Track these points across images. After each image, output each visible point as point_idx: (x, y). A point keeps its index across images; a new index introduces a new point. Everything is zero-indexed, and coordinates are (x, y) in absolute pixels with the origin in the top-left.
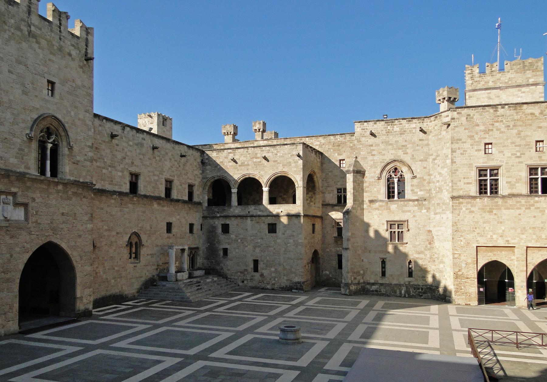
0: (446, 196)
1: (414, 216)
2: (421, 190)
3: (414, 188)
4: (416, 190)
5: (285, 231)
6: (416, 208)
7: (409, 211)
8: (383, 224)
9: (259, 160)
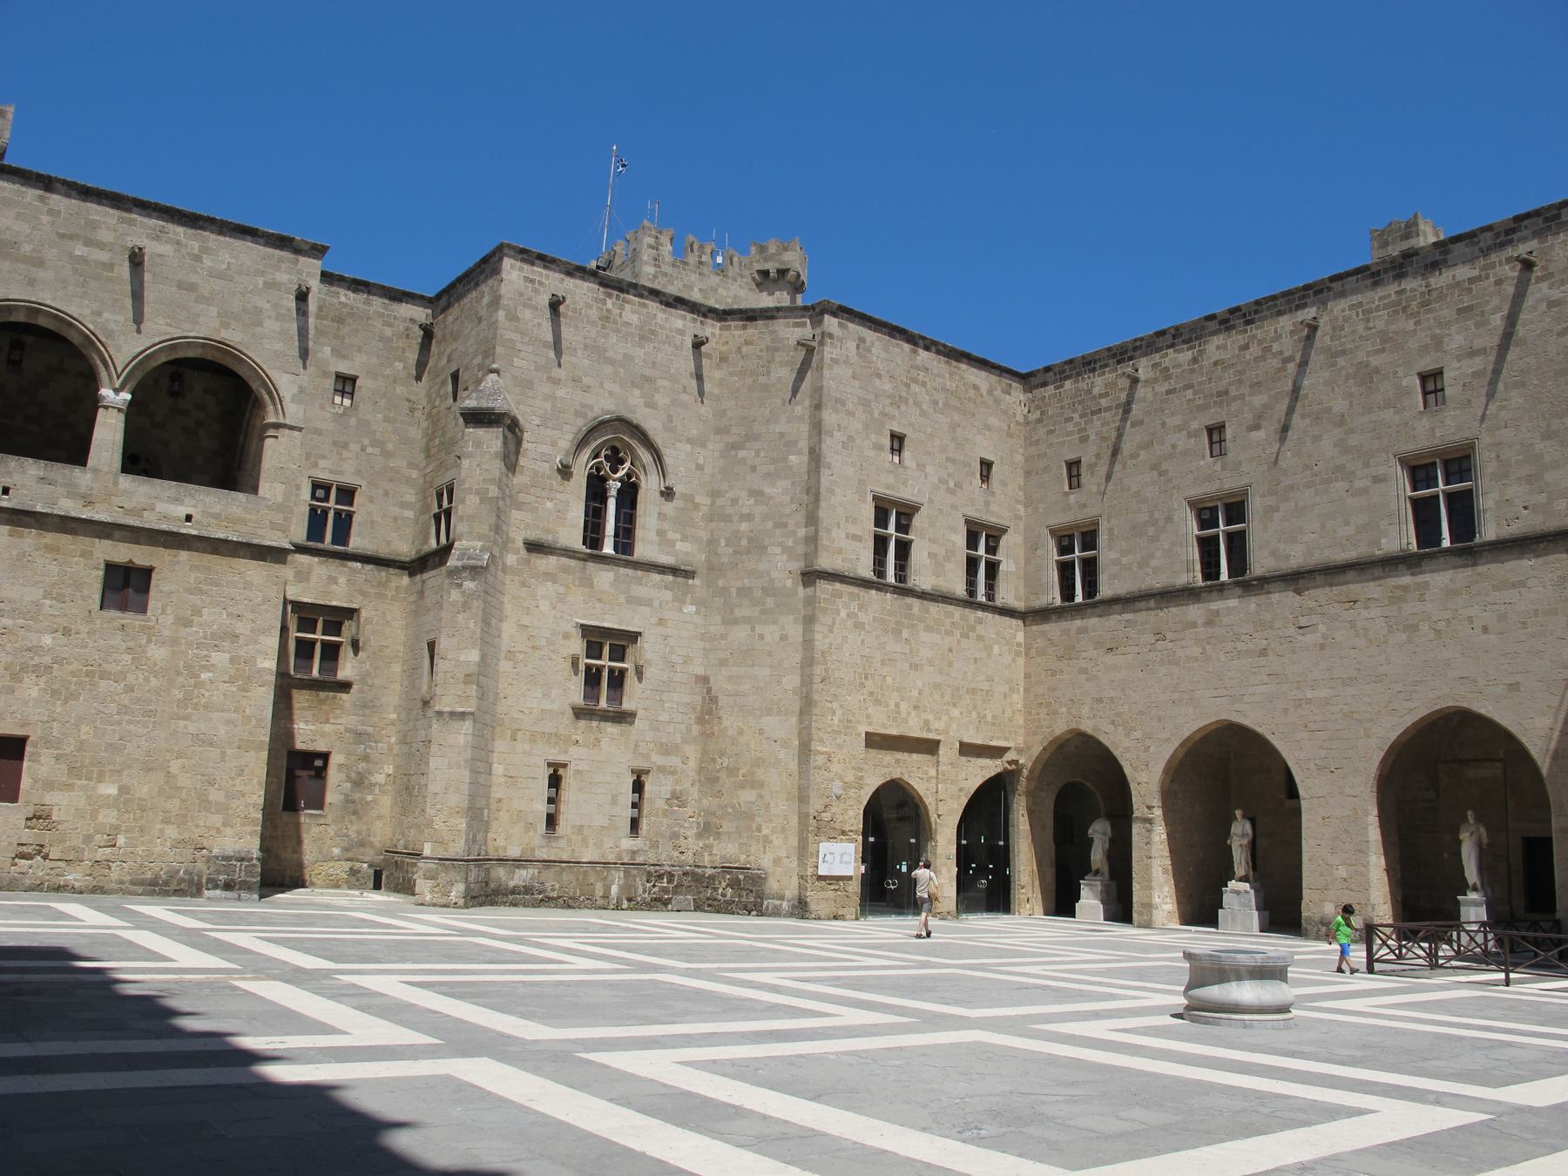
0: (782, 567)
1: (661, 622)
2: (684, 539)
3: (666, 526)
4: (671, 535)
5: (199, 613)
6: (668, 595)
7: (648, 603)
8: (567, 636)
9: (104, 256)
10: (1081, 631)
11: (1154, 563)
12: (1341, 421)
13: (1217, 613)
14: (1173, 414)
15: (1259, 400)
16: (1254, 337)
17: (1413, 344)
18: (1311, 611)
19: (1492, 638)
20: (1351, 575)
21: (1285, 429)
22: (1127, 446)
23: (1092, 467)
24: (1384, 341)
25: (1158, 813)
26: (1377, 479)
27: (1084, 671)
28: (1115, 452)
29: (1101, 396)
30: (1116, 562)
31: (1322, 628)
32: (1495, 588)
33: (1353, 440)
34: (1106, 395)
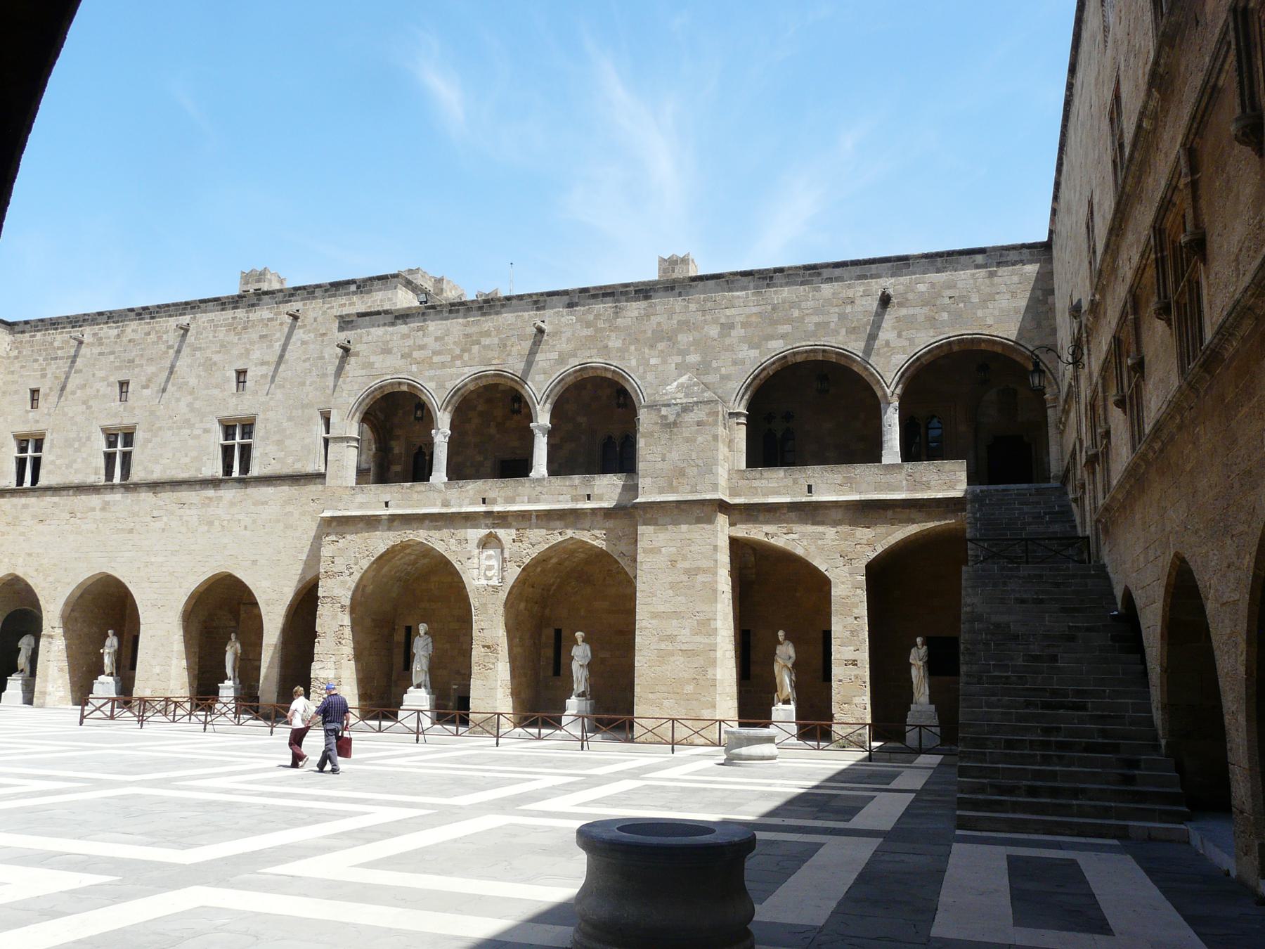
10: (25, 506)
11: (75, 466)
12: (192, 393)
13: (107, 503)
14: (100, 369)
15: (151, 369)
16: (153, 328)
17: (235, 352)
18: (160, 508)
19: (248, 533)
20: (184, 487)
21: (164, 390)
22: (69, 387)
23: (46, 395)
24: (222, 346)
25: (59, 631)
26: (206, 431)
27: (22, 534)
28: (63, 388)
29: (59, 348)
30: (53, 462)
31: (165, 519)
32: (254, 504)
33: (197, 404)
34: (61, 348)
